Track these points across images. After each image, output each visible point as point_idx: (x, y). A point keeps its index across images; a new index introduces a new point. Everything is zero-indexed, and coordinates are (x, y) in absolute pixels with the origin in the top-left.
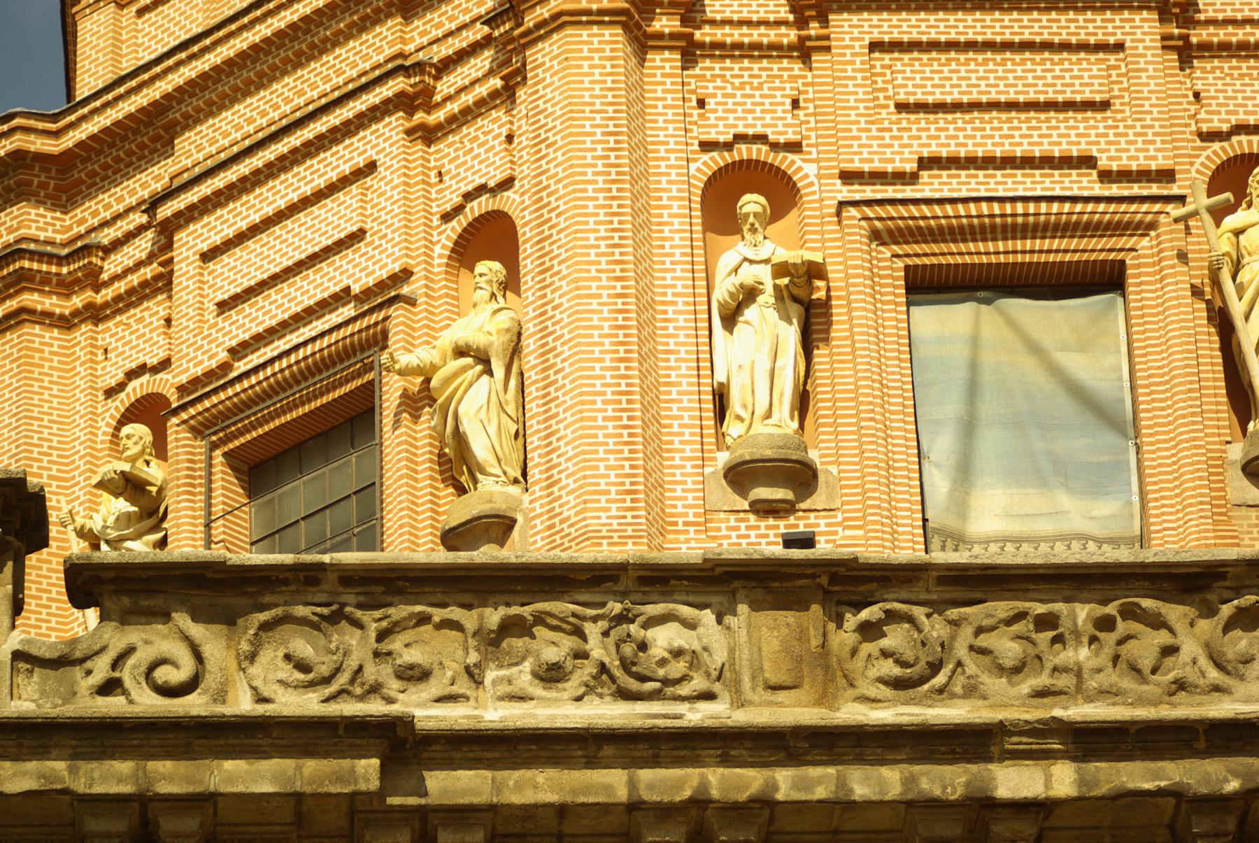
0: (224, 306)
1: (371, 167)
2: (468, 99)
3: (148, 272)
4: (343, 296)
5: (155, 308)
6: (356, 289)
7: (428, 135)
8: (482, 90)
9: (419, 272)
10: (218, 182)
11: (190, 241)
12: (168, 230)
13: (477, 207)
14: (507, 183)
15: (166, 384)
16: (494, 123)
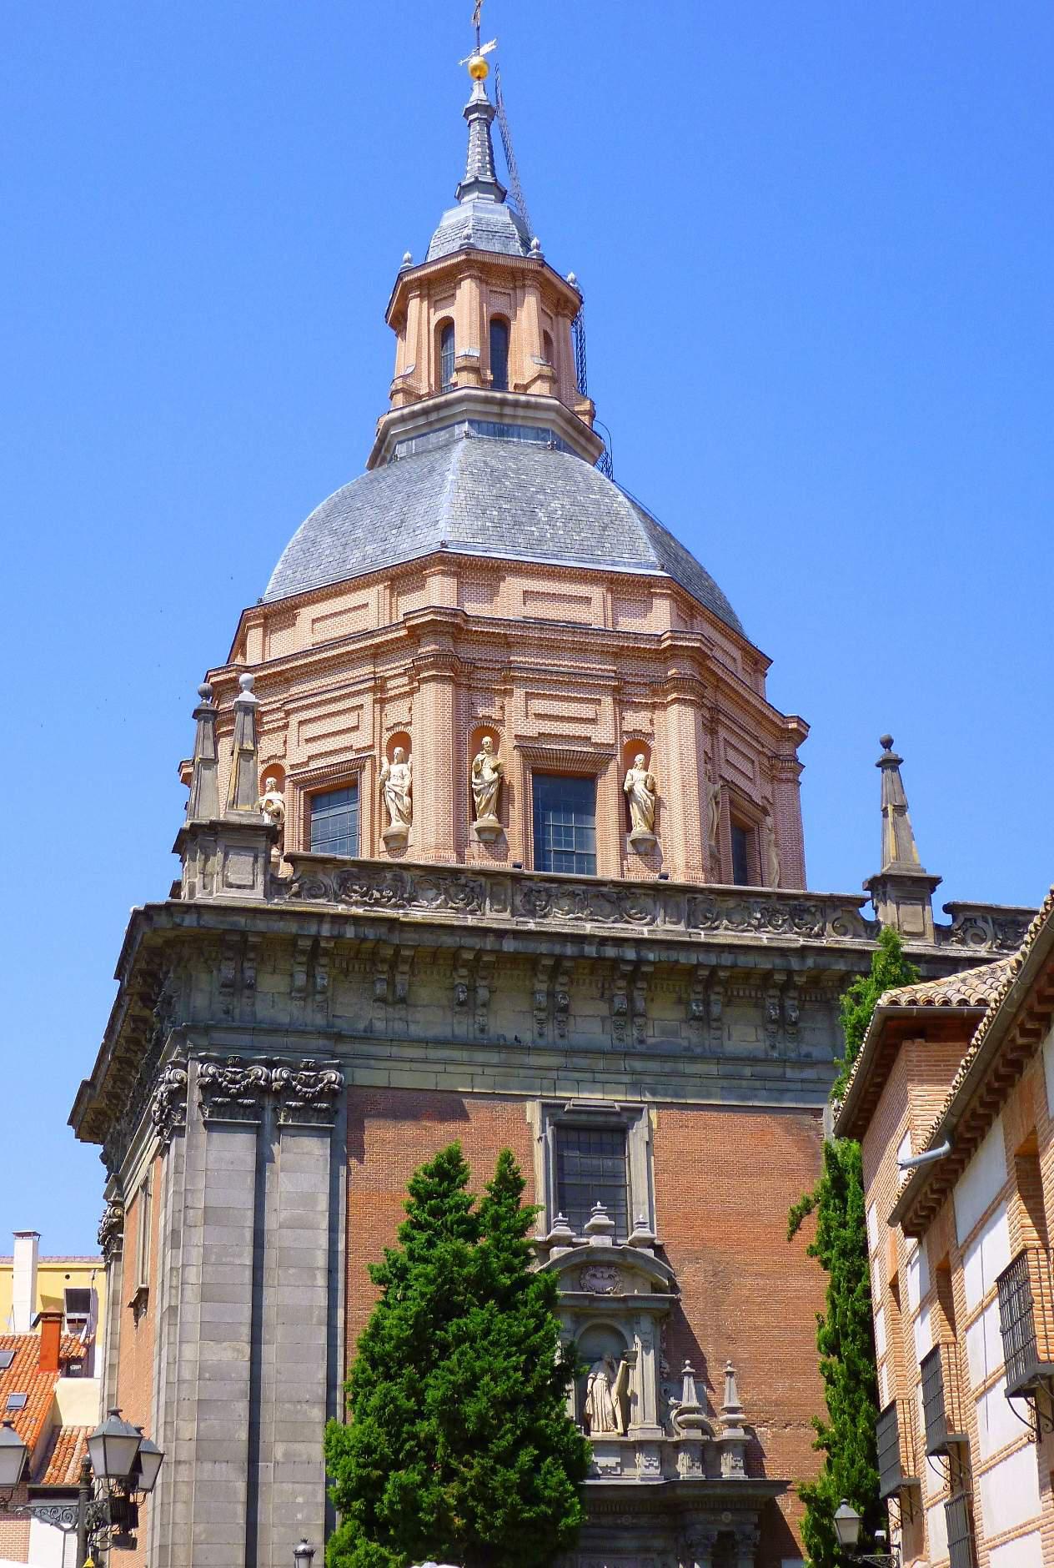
0: (308, 741)
1: (361, 707)
2: (397, 692)
3: (281, 723)
4: (349, 748)
5: (281, 734)
6: (354, 748)
7: (382, 702)
8: (402, 690)
9: (377, 745)
10: (305, 702)
11: (294, 719)
12: (288, 713)
13: (397, 729)
14: (409, 724)
15: (286, 763)
16: (403, 705)
